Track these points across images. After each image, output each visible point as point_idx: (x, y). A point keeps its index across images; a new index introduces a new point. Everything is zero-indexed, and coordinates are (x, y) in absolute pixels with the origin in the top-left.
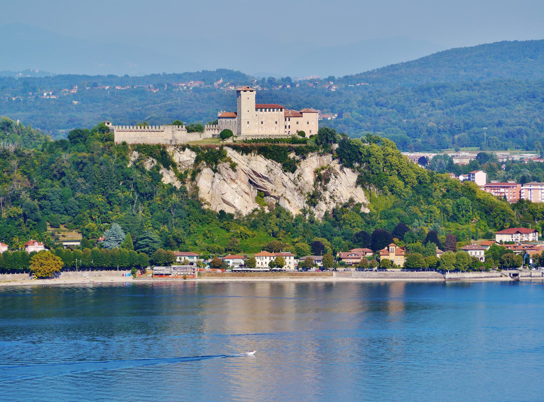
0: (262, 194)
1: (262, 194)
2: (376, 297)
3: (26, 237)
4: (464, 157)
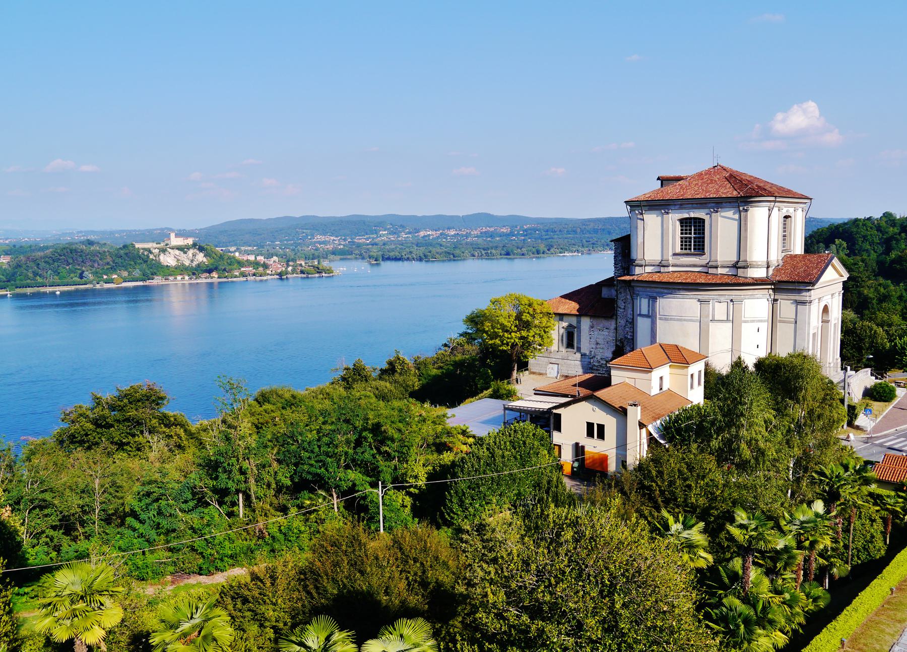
0: (178, 260)
1: (178, 260)
2: (211, 285)
3: (112, 274)
4: (233, 249)
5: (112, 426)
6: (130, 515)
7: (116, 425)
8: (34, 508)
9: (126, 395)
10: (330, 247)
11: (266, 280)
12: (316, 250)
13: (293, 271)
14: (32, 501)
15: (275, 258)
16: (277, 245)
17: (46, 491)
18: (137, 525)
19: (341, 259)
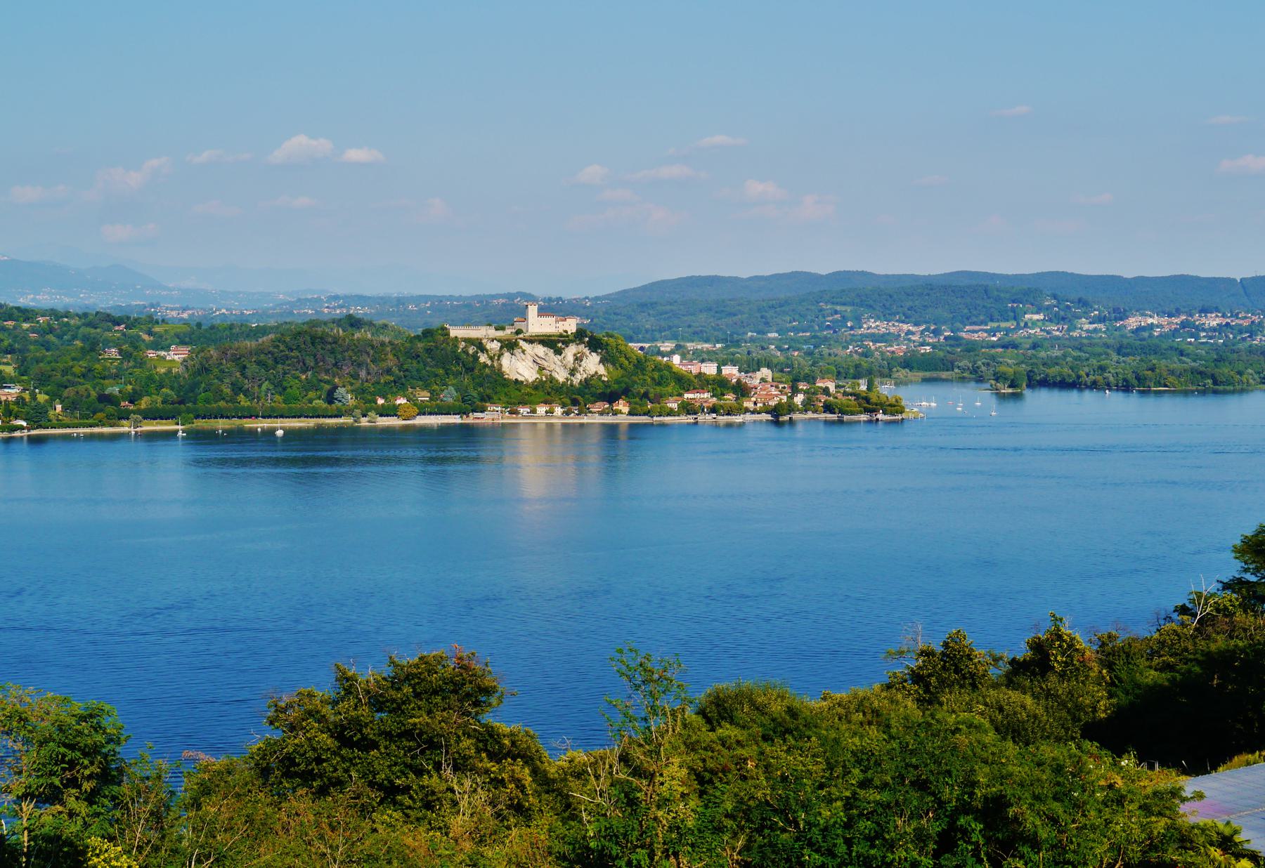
0: (541, 369)
1: (541, 369)
2: (611, 431)
3: (395, 394)
4: (667, 346)
10: (899, 349)
11: (741, 425)
12: (865, 355)
13: (808, 406)
15: (765, 372)
16: (770, 341)
19: (926, 380)
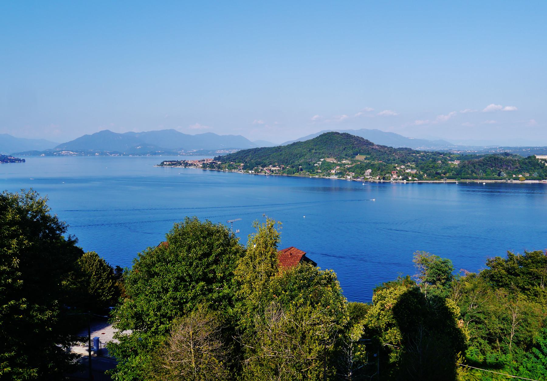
3: (519, 174)
5: (519, 275)
6: (535, 346)
7: (521, 275)
8: (472, 322)
9: (530, 257)
14: (472, 317)
17: (481, 312)
18: (541, 356)
